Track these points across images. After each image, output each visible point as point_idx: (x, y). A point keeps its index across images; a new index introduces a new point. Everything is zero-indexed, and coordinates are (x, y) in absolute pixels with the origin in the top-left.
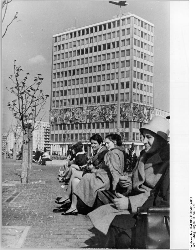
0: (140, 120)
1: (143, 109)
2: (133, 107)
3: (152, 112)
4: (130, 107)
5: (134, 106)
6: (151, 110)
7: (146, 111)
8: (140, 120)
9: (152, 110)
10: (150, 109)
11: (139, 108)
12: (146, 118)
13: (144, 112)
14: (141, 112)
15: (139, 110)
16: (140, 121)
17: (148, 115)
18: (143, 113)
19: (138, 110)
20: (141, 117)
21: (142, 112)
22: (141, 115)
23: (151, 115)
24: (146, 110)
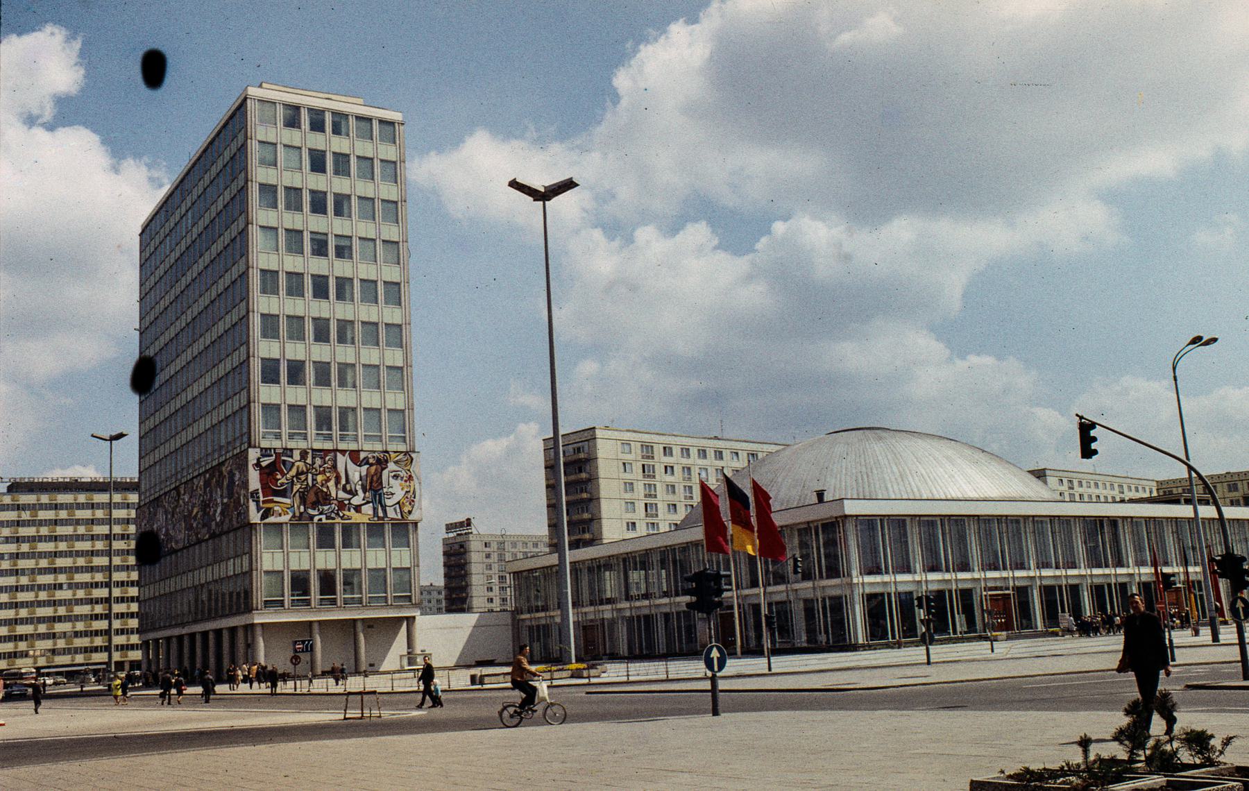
0: (311, 512)
1: (335, 467)
2: (258, 464)
3: (403, 474)
4: (247, 465)
5: (265, 462)
6: (391, 466)
7: (356, 473)
8: (311, 512)
9: (396, 462)
10: (382, 463)
11: (301, 464)
12: (356, 501)
13: (338, 479)
14: (320, 478)
15: (299, 474)
16: (312, 518)
17: (374, 487)
18: (331, 484)
19: (294, 472)
20: (325, 498)
21: (328, 480)
22: (318, 492)
23: (395, 490)
24: (351, 466)
